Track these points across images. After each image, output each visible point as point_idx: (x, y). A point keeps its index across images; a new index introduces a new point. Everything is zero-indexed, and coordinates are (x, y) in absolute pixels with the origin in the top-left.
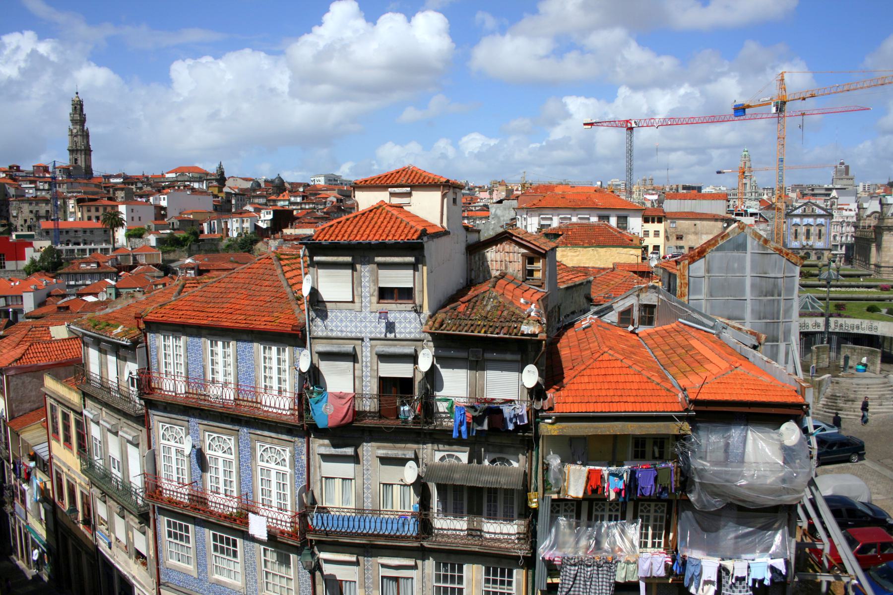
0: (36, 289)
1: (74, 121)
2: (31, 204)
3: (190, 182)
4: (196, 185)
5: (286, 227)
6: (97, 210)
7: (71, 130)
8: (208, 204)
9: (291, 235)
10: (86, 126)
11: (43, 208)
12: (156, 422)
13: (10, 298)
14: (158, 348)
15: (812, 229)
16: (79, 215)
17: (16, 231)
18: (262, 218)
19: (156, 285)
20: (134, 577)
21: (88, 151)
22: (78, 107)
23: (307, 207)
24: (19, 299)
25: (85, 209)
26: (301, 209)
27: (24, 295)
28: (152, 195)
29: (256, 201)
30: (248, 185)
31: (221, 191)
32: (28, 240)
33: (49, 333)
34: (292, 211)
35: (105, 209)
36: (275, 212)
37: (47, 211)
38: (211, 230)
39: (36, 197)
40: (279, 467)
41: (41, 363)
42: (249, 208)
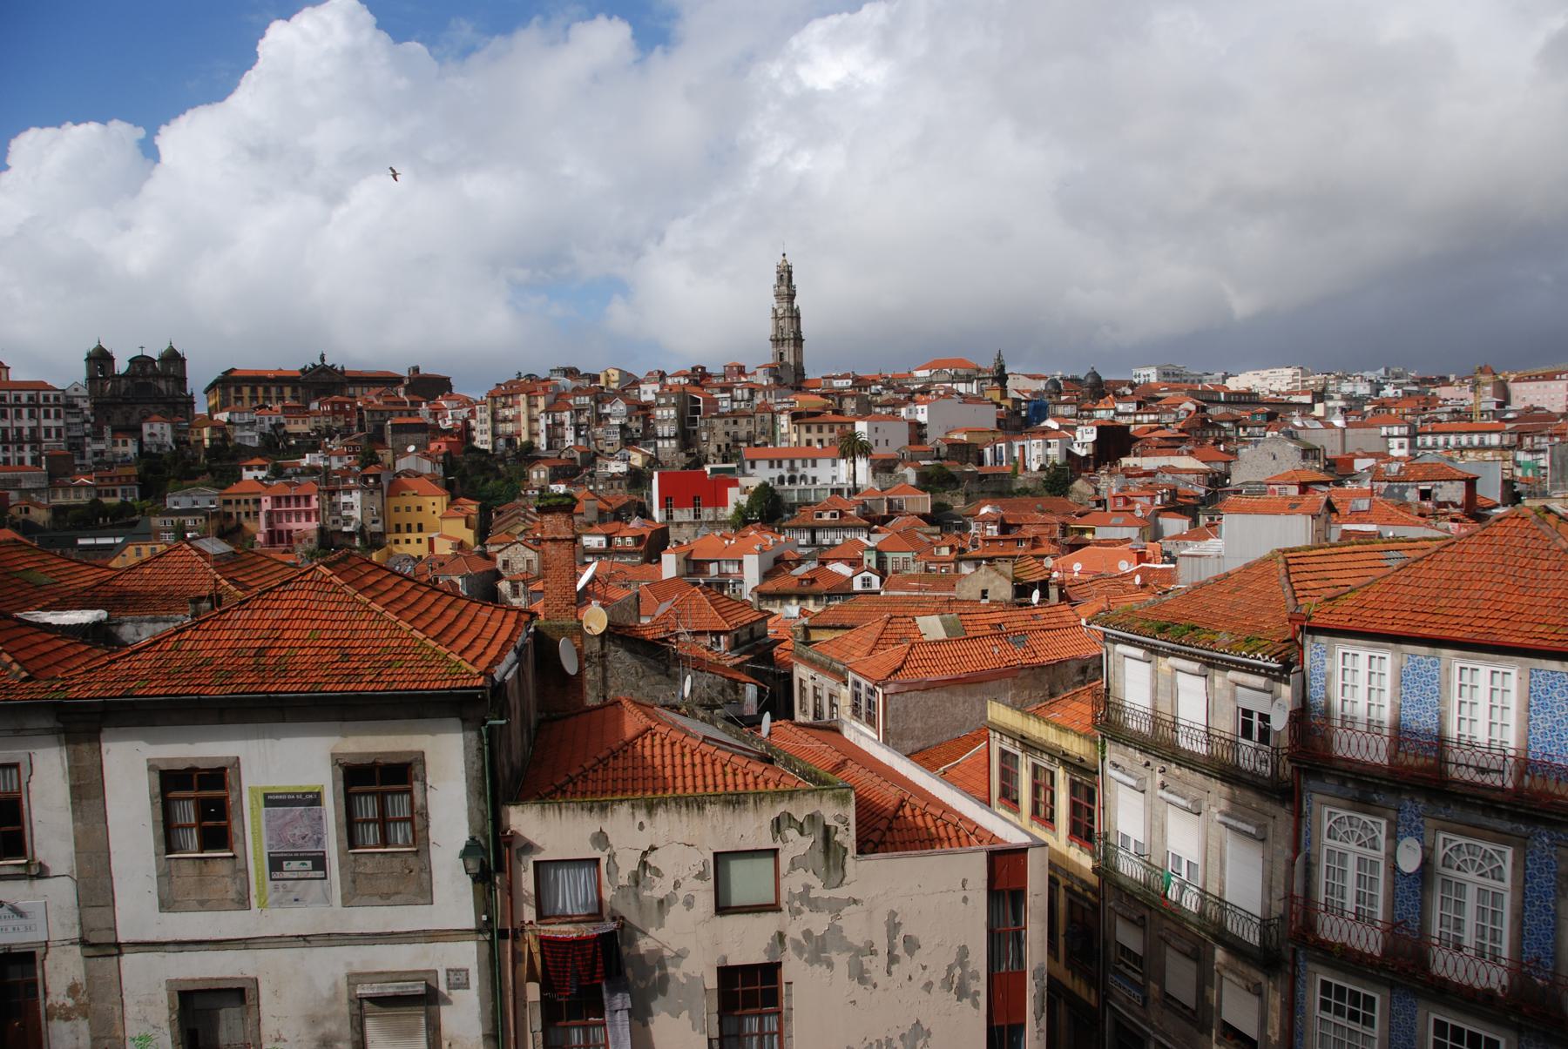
0: (762, 551)
4: (962, 388)
5: (1127, 454)
6: (820, 430)
7: (775, 311)
8: (987, 417)
9: (1136, 468)
10: (797, 302)
11: (743, 428)
12: (1315, 807)
14: (1328, 676)
16: (794, 437)
17: (707, 462)
18: (1079, 440)
21: (798, 340)
22: (786, 276)
23: (1146, 418)
26: (1136, 423)
28: (904, 404)
29: (1061, 410)
30: (1041, 385)
31: (1004, 396)
32: (731, 477)
33: (916, 627)
34: (1127, 427)
35: (832, 430)
36: (1102, 430)
38: (997, 458)
41: (932, 677)
42: (1052, 424)
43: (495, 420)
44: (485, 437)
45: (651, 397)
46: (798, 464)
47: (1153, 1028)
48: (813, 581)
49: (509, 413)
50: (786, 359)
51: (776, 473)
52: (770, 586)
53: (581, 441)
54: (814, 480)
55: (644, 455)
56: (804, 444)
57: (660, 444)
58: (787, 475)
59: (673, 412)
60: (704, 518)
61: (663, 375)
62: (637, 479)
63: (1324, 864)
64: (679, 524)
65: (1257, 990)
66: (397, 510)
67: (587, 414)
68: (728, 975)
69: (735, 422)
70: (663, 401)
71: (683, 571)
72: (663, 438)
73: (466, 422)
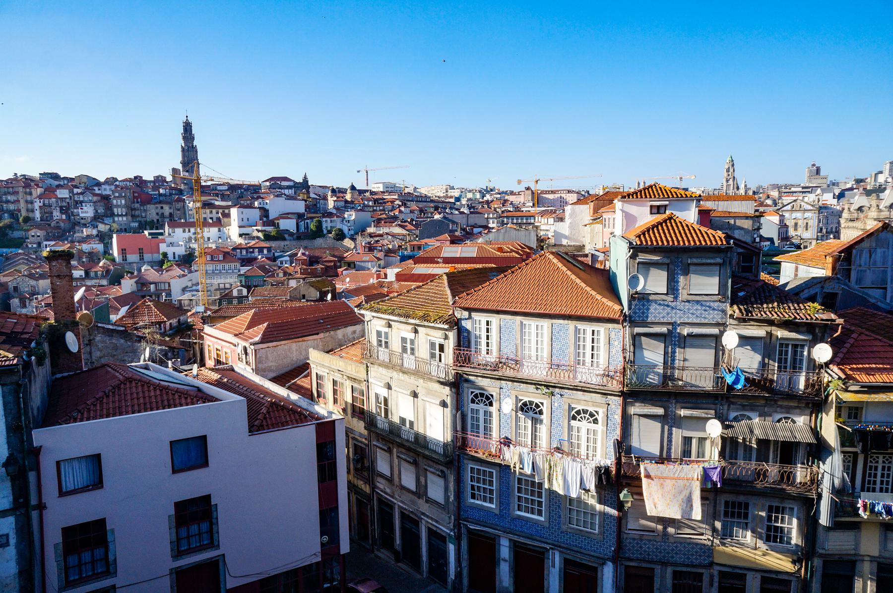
1: (184, 138)
2: (157, 208)
6: (211, 212)
11: (167, 210)
12: (466, 390)
15: (800, 223)
20: (423, 514)
22: (188, 128)
24: (167, 285)
27: (173, 282)
35: (217, 213)
40: (592, 426)
45: (108, 192)
47: (396, 499)
57: (116, 219)
58: (193, 236)
59: (123, 202)
61: (115, 180)
63: (470, 415)
65: (443, 475)
68: (180, 506)
69: (162, 208)
71: (134, 288)
72: (118, 215)
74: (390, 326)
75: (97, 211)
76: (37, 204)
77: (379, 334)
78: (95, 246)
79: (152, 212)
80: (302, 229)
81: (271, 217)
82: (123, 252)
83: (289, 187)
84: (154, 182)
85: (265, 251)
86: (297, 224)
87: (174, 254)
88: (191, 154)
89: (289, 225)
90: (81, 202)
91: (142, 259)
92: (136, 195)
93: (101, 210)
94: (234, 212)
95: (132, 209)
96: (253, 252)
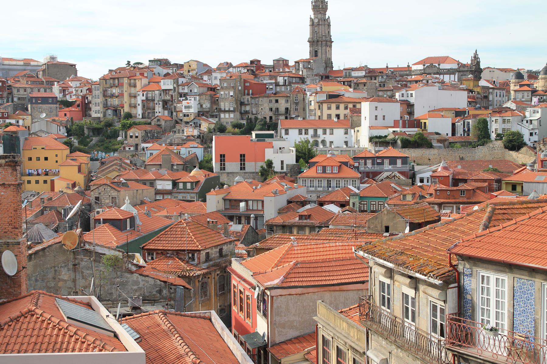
2: (270, 101)
3: (440, 74)
6: (338, 108)
8: (460, 100)
10: (328, 14)
11: (283, 105)
13: (250, 203)
19: (404, 196)
21: (328, 42)
24: (260, 204)
25: (325, 106)
27: (266, 199)
28: (398, 89)
35: (346, 108)
37: (287, 109)
39: (275, 94)
43: (105, 96)
44: (98, 108)
46: (320, 132)
48: (309, 217)
49: (116, 91)
50: (319, 54)
51: (303, 137)
52: (280, 221)
53: (166, 112)
54: (331, 142)
55: (211, 123)
56: (325, 117)
57: (222, 115)
58: (311, 140)
59: (232, 93)
60: (247, 170)
61: (230, 65)
62: (204, 140)
64: (228, 173)
66: (30, 159)
67: (171, 93)
69: (277, 101)
70: (225, 85)
71: (221, 206)
72: (225, 111)
73: (84, 97)
74: (391, 277)
75: (201, 106)
76: (140, 98)
77: (382, 284)
78: (194, 150)
79: (263, 109)
80: (460, 131)
81: (417, 114)
82: (222, 158)
83: (450, 72)
84: (273, 67)
85: (399, 162)
86: (453, 125)
87: (282, 162)
88: (322, 30)
89: (440, 126)
90: (185, 95)
91: (243, 168)
92: (247, 84)
93: (207, 105)
94: (365, 107)
95: (242, 104)
96: (382, 163)
